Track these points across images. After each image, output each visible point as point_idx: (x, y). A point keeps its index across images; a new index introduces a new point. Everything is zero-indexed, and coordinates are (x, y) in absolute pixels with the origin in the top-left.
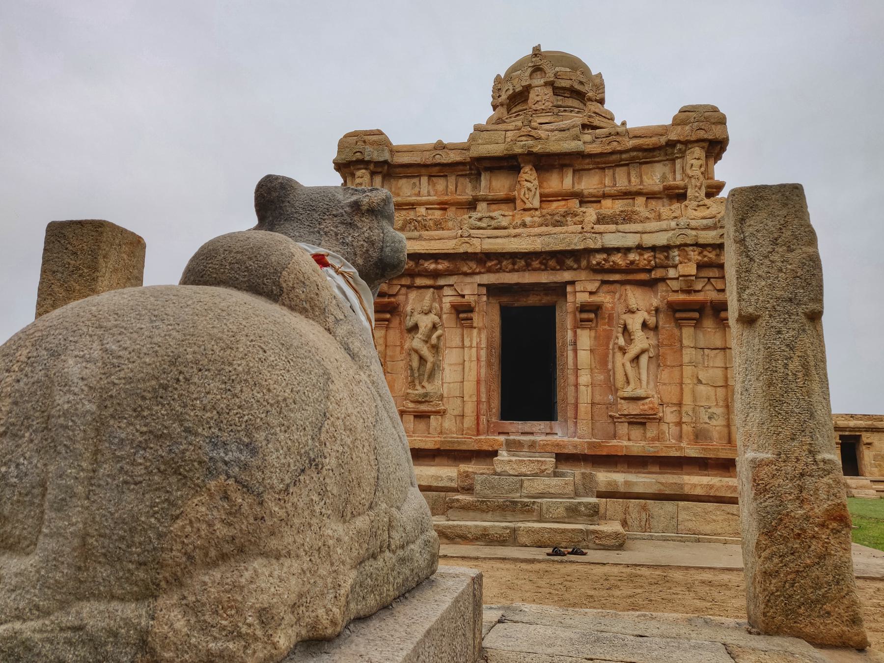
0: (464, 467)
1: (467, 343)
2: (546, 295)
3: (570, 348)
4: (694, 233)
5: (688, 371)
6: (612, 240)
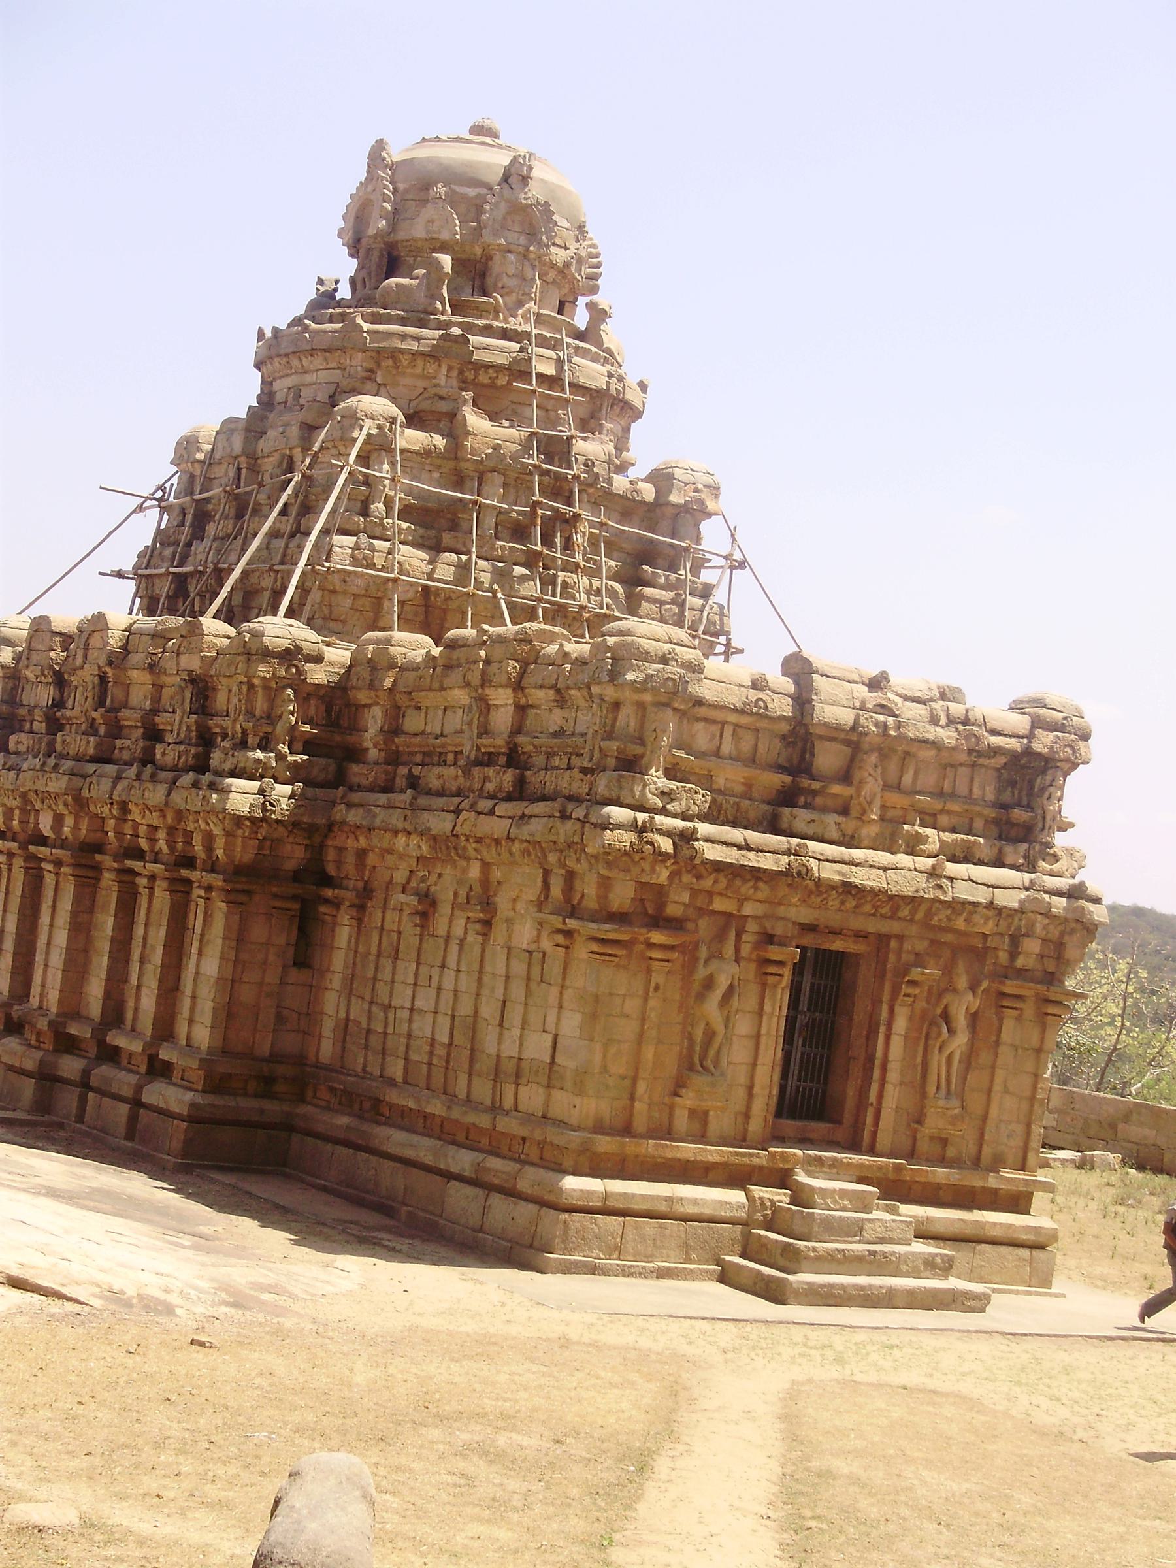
0: (758, 1191)
1: (767, 1008)
2: (855, 942)
3: (882, 1029)
4: (1046, 897)
5: (1000, 1075)
6: (963, 892)
